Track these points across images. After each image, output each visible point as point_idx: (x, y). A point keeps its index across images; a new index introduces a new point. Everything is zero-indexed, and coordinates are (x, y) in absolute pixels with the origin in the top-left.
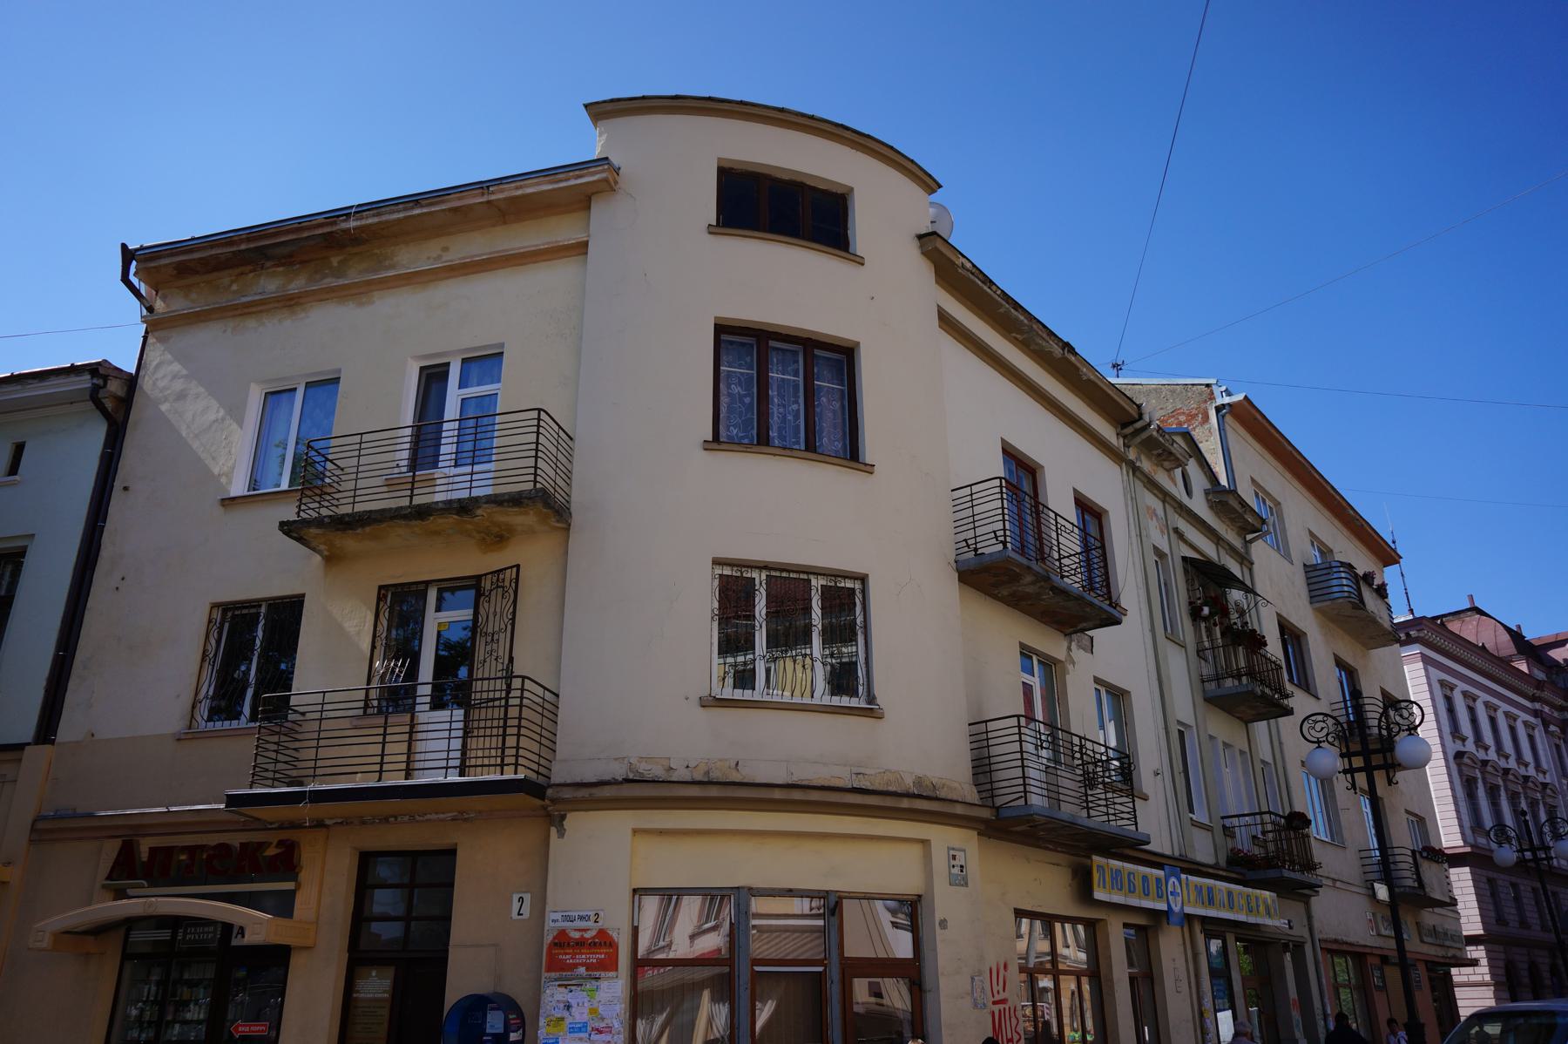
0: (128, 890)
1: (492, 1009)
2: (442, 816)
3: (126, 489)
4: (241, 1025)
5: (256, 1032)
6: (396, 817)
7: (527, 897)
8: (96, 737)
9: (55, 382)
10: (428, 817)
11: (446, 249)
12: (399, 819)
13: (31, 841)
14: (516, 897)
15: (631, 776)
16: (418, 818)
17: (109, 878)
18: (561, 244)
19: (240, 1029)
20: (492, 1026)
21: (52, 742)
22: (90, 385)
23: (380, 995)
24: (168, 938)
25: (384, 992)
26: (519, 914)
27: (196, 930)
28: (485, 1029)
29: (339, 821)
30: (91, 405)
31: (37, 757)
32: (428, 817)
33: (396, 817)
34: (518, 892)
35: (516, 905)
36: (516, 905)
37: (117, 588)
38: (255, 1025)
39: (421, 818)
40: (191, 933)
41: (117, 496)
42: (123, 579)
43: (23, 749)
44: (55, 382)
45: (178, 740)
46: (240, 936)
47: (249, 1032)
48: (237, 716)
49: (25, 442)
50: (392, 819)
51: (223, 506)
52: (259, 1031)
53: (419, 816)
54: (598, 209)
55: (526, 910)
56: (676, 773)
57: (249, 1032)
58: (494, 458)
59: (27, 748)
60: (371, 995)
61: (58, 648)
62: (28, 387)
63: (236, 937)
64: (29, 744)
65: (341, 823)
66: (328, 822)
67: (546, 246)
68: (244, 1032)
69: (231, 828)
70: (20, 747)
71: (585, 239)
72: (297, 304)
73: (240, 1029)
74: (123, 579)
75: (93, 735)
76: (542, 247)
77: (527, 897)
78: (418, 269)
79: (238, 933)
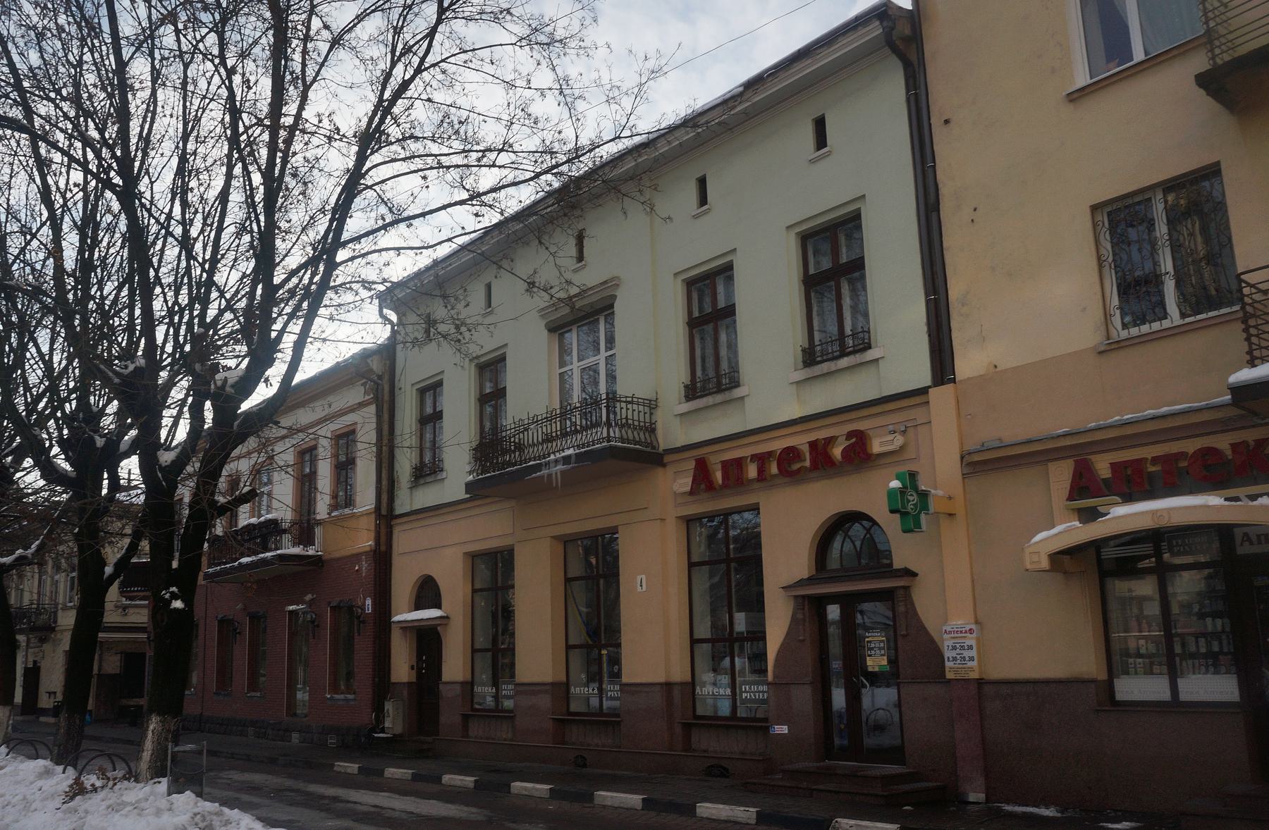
3: (947, 122)
8: (997, 370)
9: (844, 42)
13: (963, 474)
17: (1070, 498)
21: (954, 381)
22: (881, 30)
27: (1177, 543)
30: (887, 50)
31: (942, 397)
37: (972, 220)
41: (939, 133)
42: (975, 210)
43: (928, 393)
44: (844, 42)
45: (1100, 353)
48: (1165, 316)
49: (824, 114)
59: (930, 390)
61: (927, 295)
62: (818, 57)
63: (1242, 545)
64: (930, 387)
70: (923, 391)
74: (975, 210)
75: (996, 367)
79: (1243, 540)
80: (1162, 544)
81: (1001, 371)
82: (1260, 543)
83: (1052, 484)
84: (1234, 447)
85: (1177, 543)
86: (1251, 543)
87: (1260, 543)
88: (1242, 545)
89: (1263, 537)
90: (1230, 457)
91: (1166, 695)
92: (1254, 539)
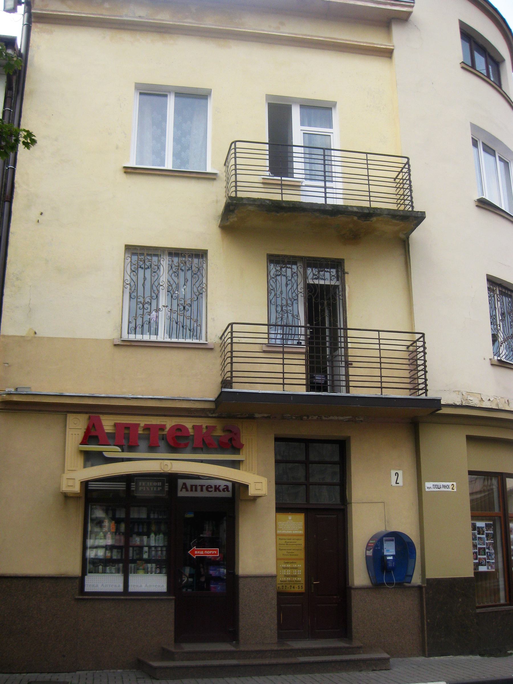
0: (104, 452)
1: (386, 540)
2: (341, 418)
4: (197, 550)
5: (209, 554)
6: (308, 417)
7: (400, 473)
8: (36, 336)
10: (331, 418)
11: (282, 24)
12: (310, 418)
14: (393, 472)
15: (464, 404)
16: (324, 418)
18: (375, 46)
19: (196, 552)
20: (388, 551)
23: (296, 532)
24: (124, 488)
25: (300, 530)
26: (396, 483)
27: (142, 484)
28: (384, 553)
29: (266, 415)
32: (331, 418)
33: (308, 417)
34: (394, 469)
35: (394, 478)
36: (394, 478)
38: (207, 550)
39: (326, 418)
40: (142, 486)
42: (41, 214)
46: (184, 490)
47: (204, 554)
50: (305, 417)
51: (125, 172)
52: (211, 554)
53: (325, 417)
54: (397, 31)
55: (400, 480)
56: (484, 403)
57: (204, 554)
58: (334, 179)
60: (290, 532)
63: (181, 491)
65: (268, 417)
66: (257, 415)
67: (365, 44)
68: (200, 554)
69: (160, 414)
71: (392, 48)
72: (165, 32)
73: (196, 552)
74: (41, 214)
75: (35, 333)
76: (362, 44)
77: (400, 473)
78: (270, 33)
79: (182, 488)
80: (132, 484)
81: (39, 337)
82: (192, 490)
83: (68, 430)
84: (194, 427)
85: (142, 484)
86: (187, 490)
87: (192, 490)
88: (181, 491)
89: (194, 487)
90: (192, 434)
91: (120, 588)
92: (189, 488)
